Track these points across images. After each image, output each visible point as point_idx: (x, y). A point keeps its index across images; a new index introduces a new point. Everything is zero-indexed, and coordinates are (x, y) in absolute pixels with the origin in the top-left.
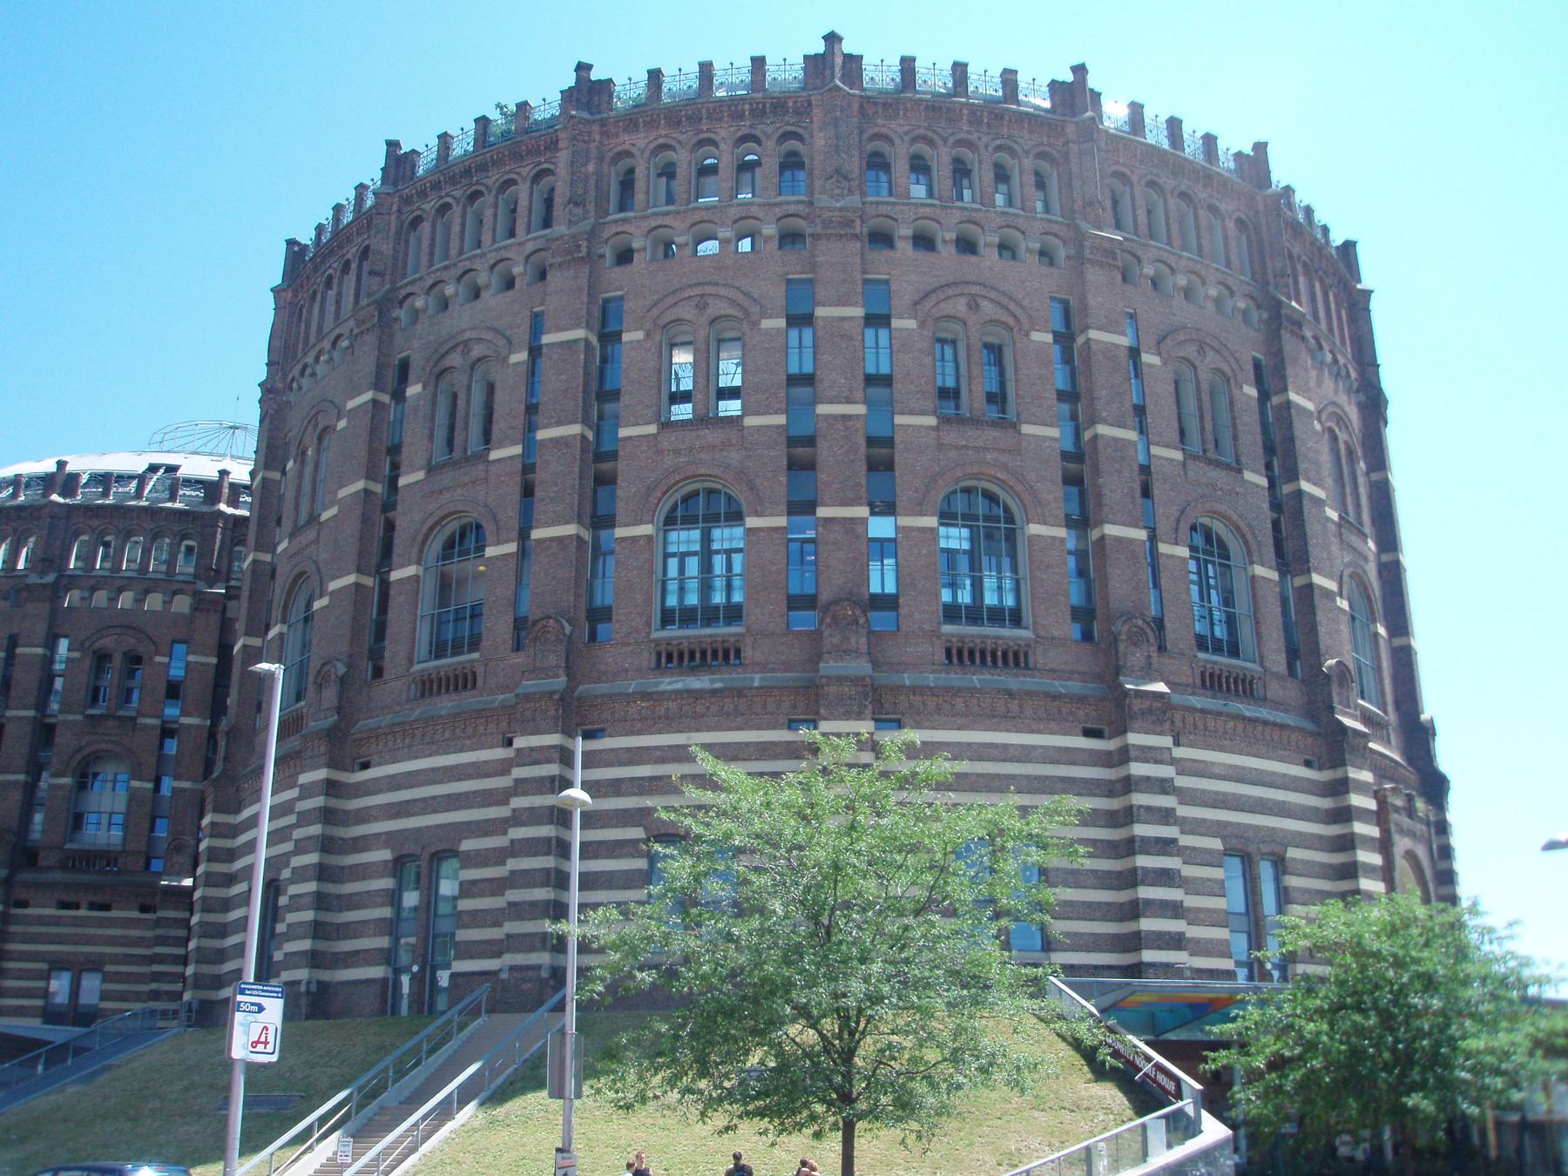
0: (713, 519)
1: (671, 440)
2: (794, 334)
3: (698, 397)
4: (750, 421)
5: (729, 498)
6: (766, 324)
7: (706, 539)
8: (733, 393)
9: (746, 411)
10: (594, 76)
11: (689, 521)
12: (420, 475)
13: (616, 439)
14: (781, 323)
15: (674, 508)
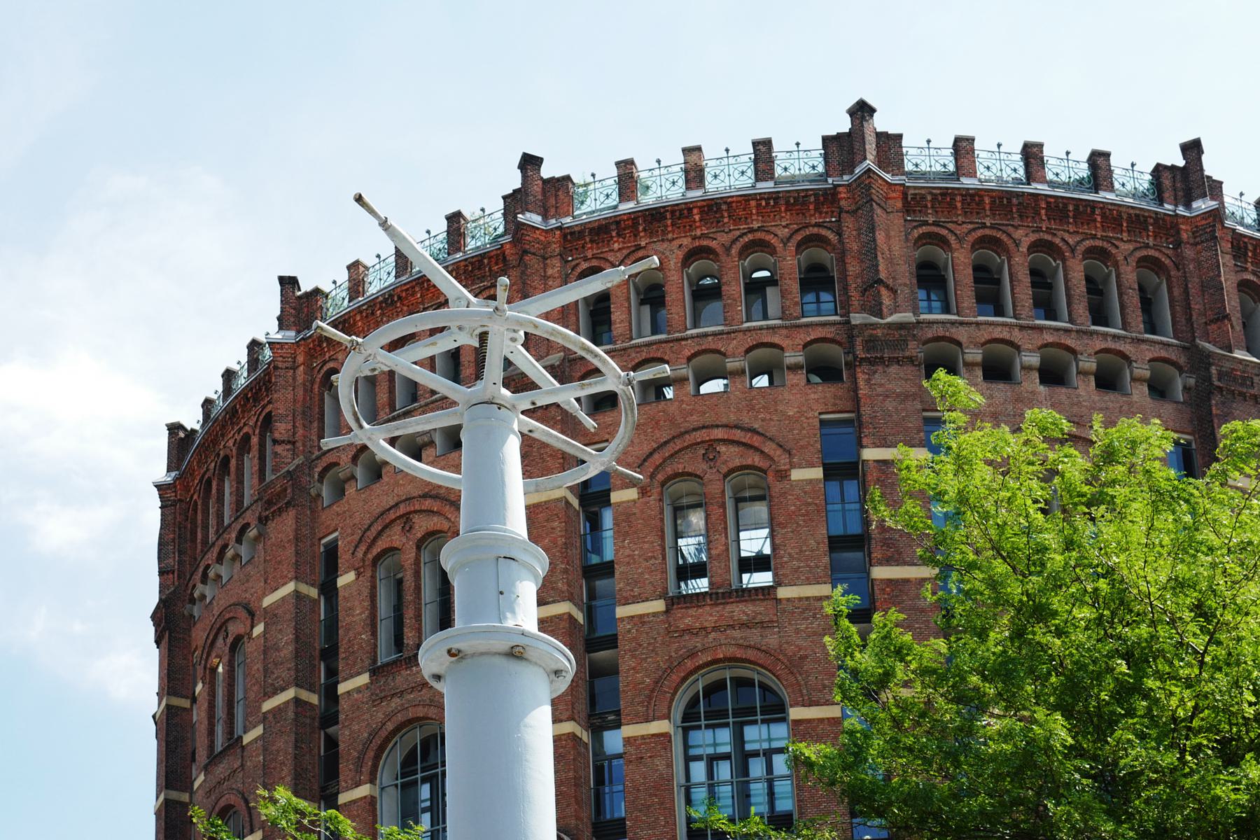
0: (745, 715)
1: (688, 618)
2: (834, 487)
3: (714, 567)
4: (783, 593)
5: (764, 688)
6: (797, 475)
7: (739, 739)
8: (759, 563)
9: (778, 583)
10: (547, 172)
11: (716, 718)
12: (364, 679)
13: (614, 620)
14: (817, 473)
15: (694, 702)
